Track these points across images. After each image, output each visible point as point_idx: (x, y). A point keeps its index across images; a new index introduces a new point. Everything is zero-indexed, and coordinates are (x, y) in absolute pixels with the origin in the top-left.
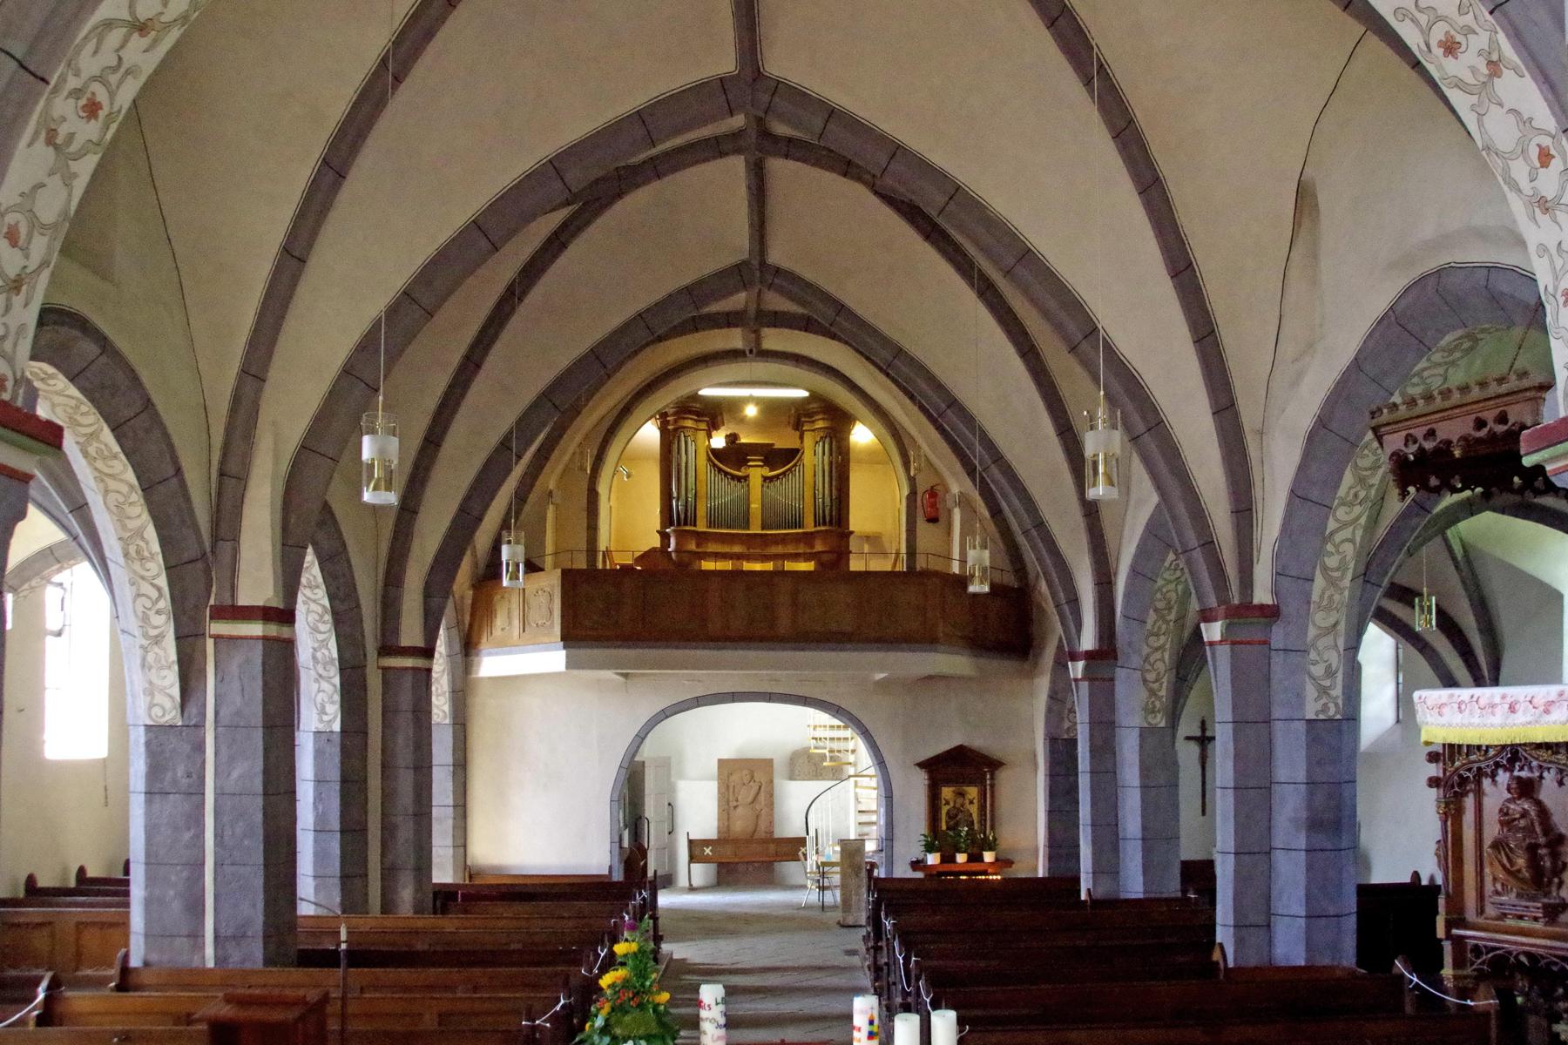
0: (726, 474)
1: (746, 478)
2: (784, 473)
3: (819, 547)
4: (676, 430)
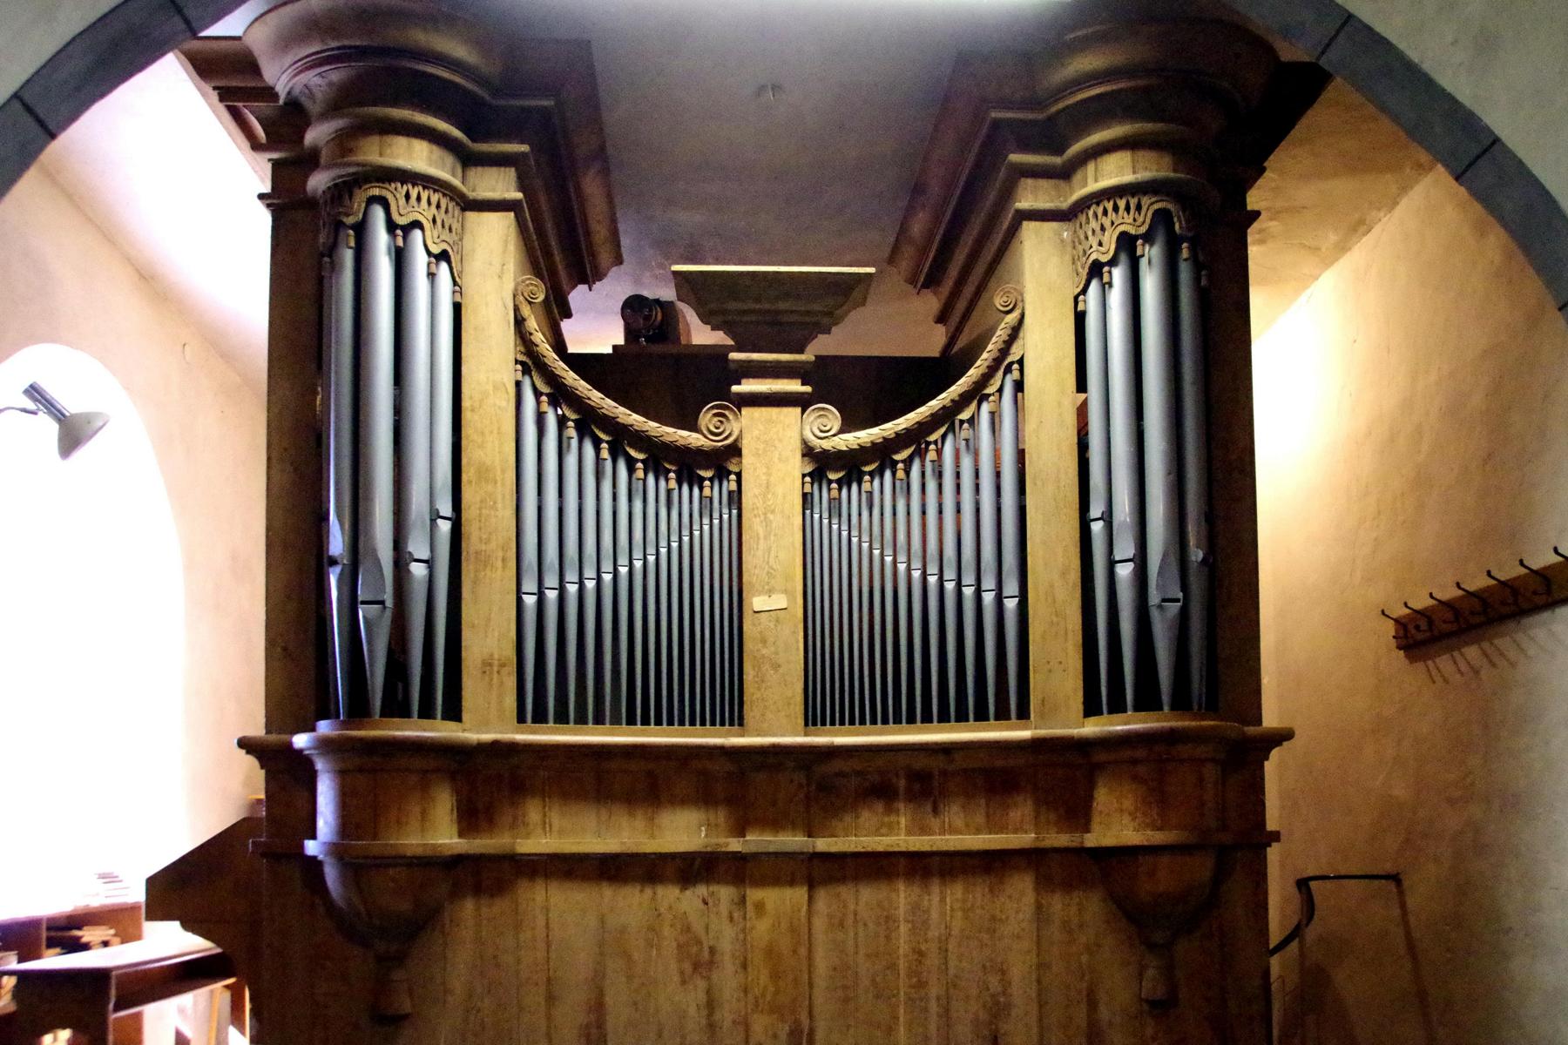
0: (622, 438)
1: (723, 460)
2: (915, 438)
3: (1117, 823)
4: (342, 191)
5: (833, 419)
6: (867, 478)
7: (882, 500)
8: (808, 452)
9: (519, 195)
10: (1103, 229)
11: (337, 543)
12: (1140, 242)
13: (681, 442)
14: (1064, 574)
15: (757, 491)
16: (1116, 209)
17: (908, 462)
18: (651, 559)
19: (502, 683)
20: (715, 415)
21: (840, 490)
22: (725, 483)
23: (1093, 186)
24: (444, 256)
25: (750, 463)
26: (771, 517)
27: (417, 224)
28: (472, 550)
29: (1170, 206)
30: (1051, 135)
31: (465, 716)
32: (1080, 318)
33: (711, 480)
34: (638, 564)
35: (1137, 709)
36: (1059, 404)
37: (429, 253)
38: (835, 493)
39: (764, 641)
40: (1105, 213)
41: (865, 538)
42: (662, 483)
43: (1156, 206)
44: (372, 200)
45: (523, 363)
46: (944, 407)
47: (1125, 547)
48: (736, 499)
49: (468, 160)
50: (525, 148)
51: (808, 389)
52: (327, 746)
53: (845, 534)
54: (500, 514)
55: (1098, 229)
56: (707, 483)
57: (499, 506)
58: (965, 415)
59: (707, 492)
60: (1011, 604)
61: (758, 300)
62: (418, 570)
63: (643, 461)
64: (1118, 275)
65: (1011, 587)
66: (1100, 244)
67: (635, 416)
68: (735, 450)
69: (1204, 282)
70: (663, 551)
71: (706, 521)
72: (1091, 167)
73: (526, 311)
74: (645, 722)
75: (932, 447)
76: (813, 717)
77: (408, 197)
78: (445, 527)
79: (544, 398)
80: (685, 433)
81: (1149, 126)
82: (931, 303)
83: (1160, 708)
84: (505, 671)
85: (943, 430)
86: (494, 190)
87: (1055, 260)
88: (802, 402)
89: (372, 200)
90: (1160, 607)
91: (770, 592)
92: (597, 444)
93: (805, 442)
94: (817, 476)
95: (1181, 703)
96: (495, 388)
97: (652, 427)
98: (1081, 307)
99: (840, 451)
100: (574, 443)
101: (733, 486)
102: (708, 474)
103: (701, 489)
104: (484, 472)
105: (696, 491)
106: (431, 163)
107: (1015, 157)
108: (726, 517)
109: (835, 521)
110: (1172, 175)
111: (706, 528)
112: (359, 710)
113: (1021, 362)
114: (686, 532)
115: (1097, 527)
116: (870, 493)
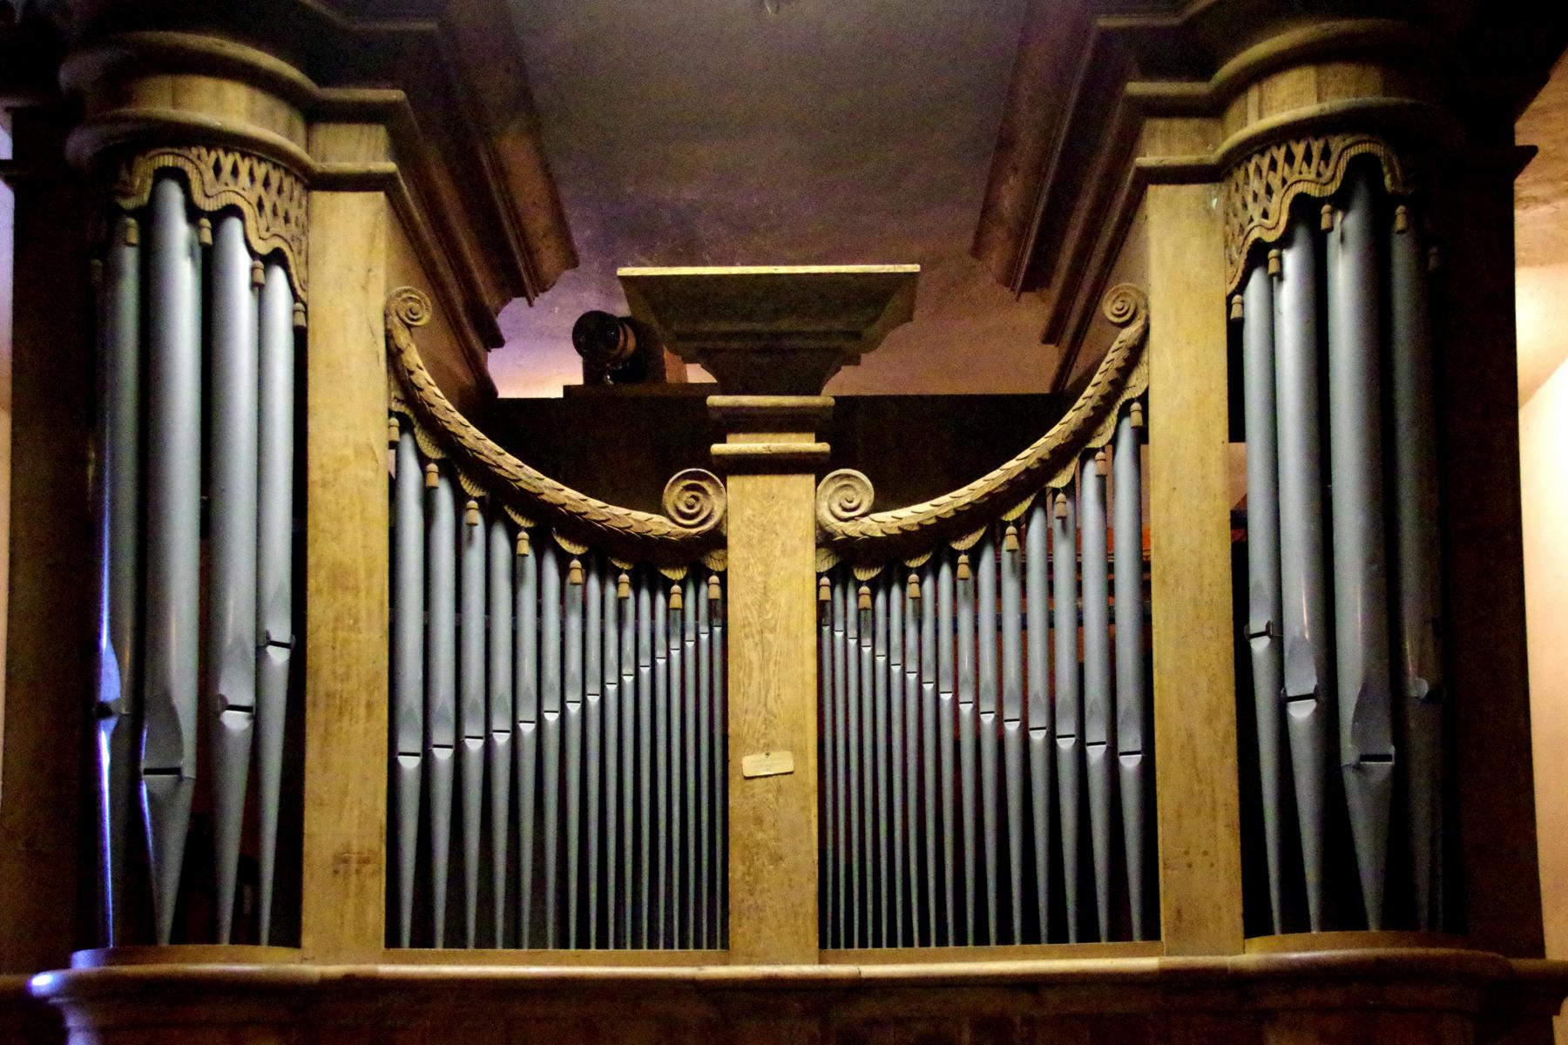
0: (549, 525)
1: (701, 553)
2: (986, 518)
5: (862, 490)
6: (913, 577)
7: (936, 610)
8: (825, 540)
9: (391, 166)
11: (112, 686)
13: (636, 529)
14: (1210, 719)
15: (749, 600)
16: (1290, 158)
17: (975, 555)
18: (593, 701)
19: (361, 889)
20: (687, 488)
21: (873, 597)
22: (703, 588)
23: (1255, 126)
24: (276, 258)
25: (738, 557)
26: (769, 636)
27: (233, 211)
28: (322, 690)
29: (1378, 150)
30: (1191, 51)
31: (307, 940)
32: (1235, 330)
33: (683, 583)
34: (574, 709)
35: (1324, 927)
37: (253, 253)
38: (866, 601)
39: (759, 821)
40: (1273, 165)
41: (912, 666)
42: (611, 589)
43: (1353, 152)
44: (163, 174)
45: (399, 415)
46: (1027, 470)
47: (1302, 678)
48: (718, 611)
49: (314, 114)
50: (396, 95)
51: (824, 447)
52: (80, 990)
53: (881, 660)
54: (363, 636)
55: (1262, 192)
56: (676, 588)
57: (363, 625)
58: (1060, 481)
59: (676, 601)
60: (1130, 764)
61: (748, 317)
62: (236, 722)
63: (580, 558)
64: (1292, 261)
65: (1130, 739)
66: (1265, 215)
67: (568, 491)
68: (716, 540)
69: (1432, 262)
70: (612, 689)
71: (675, 644)
72: (1253, 95)
73: (402, 338)
74: (583, 943)
75: (1011, 529)
76: (831, 937)
77: (217, 169)
78: (279, 658)
79: (433, 467)
80: (641, 515)
81: (1344, 25)
82: (1033, 314)
83: (1365, 927)
84: (368, 868)
85: (1026, 505)
86: (353, 158)
87: (1196, 243)
88: (813, 466)
89: (163, 174)
90: (1358, 768)
91: (768, 749)
92: (512, 532)
93: (820, 527)
94: (840, 576)
95: (1397, 917)
96: (358, 454)
97: (593, 507)
98: (1235, 313)
99: (873, 538)
100: (479, 532)
101: (715, 592)
102: (678, 575)
103: (668, 597)
104: (341, 579)
105: (661, 599)
106: (252, 116)
107: (1136, 88)
108: (704, 637)
109: (867, 641)
110: (1382, 100)
111: (675, 654)
112: (139, 933)
113: (1144, 399)
114: (645, 661)
115: (1260, 646)
116: (919, 601)
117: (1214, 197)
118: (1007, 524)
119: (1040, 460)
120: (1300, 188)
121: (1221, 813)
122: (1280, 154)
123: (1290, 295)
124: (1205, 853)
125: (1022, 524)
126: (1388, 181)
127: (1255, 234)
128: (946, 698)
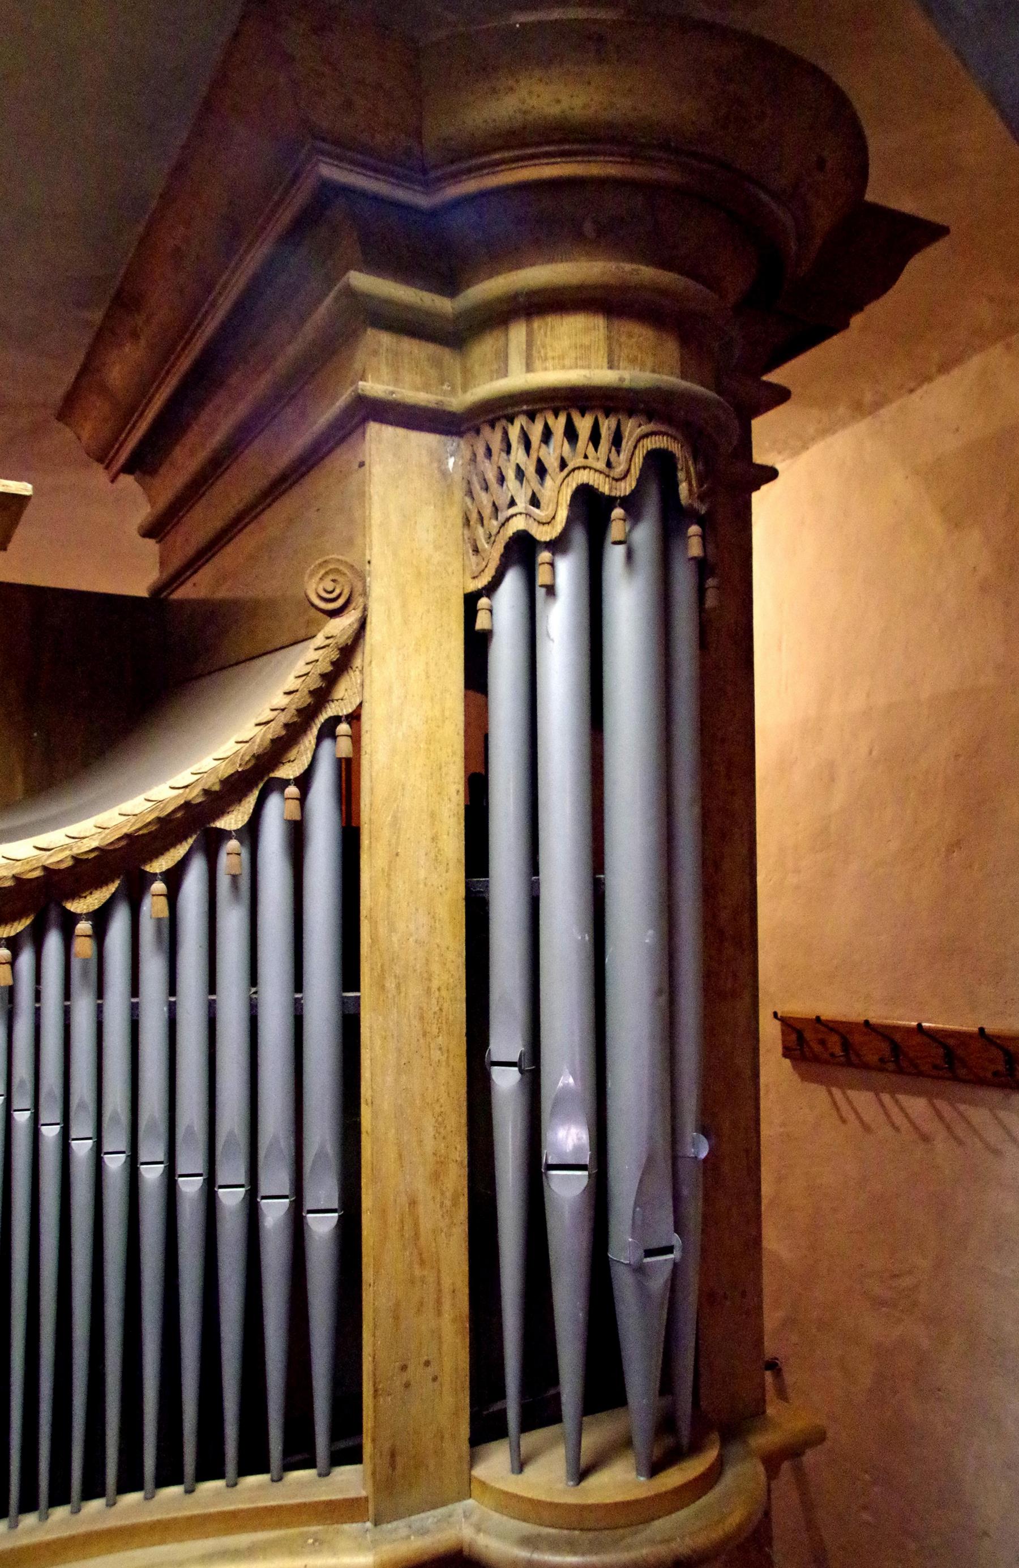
7: (37, 1013)
10: (541, 470)
12: (618, 512)
14: (436, 1177)
17: (101, 919)
23: (519, 379)
29: (675, 448)
32: (477, 646)
36: (433, 815)
40: (547, 435)
43: (650, 444)
46: (187, 805)
55: (530, 470)
58: (233, 820)
60: (322, 1227)
64: (566, 572)
65: (323, 1190)
72: (518, 333)
75: (159, 887)
81: (648, 273)
82: (135, 503)
85: (179, 852)
87: (428, 516)
98: (482, 622)
113: (354, 718)
115: (506, 1081)
117: (453, 456)
118: (154, 877)
119: (206, 792)
120: (583, 477)
121: (447, 1306)
122: (558, 426)
123: (560, 620)
124: (427, 1363)
125: (174, 878)
126: (683, 488)
127: (518, 524)
128: (50, 1133)
